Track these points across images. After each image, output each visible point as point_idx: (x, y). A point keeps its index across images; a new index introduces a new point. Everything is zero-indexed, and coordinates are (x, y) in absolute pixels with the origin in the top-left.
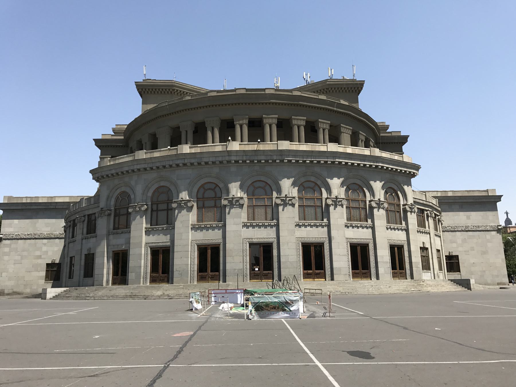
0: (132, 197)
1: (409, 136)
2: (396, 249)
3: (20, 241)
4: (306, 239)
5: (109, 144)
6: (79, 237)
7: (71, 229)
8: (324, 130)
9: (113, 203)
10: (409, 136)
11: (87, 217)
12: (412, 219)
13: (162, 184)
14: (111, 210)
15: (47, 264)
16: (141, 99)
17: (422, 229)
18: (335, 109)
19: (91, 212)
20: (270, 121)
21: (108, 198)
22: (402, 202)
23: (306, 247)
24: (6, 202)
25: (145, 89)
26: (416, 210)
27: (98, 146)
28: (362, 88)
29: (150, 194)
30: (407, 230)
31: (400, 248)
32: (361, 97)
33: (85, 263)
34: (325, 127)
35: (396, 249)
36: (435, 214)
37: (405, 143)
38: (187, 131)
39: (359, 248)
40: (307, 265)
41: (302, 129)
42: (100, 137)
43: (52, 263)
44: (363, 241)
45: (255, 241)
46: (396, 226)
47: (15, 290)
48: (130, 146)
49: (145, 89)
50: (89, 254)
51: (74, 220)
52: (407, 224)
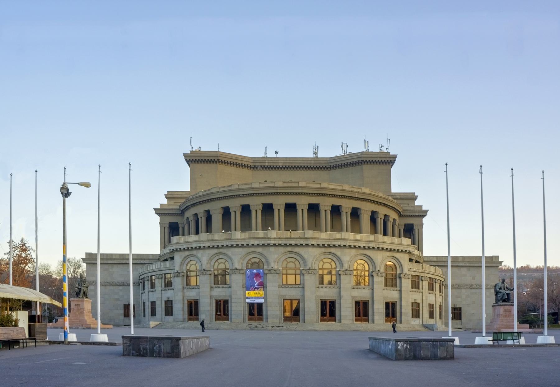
1: (428, 210)
5: (166, 212)
9: (184, 268)
10: (428, 210)
12: (406, 284)
16: (189, 168)
17: (414, 290)
21: (181, 264)
22: (398, 273)
23: (323, 303)
25: (195, 160)
26: (410, 277)
28: (395, 161)
29: (212, 264)
30: (400, 291)
31: (394, 304)
32: (395, 170)
37: (425, 216)
42: (158, 207)
44: (365, 299)
46: (392, 288)
49: (195, 160)
52: (401, 287)
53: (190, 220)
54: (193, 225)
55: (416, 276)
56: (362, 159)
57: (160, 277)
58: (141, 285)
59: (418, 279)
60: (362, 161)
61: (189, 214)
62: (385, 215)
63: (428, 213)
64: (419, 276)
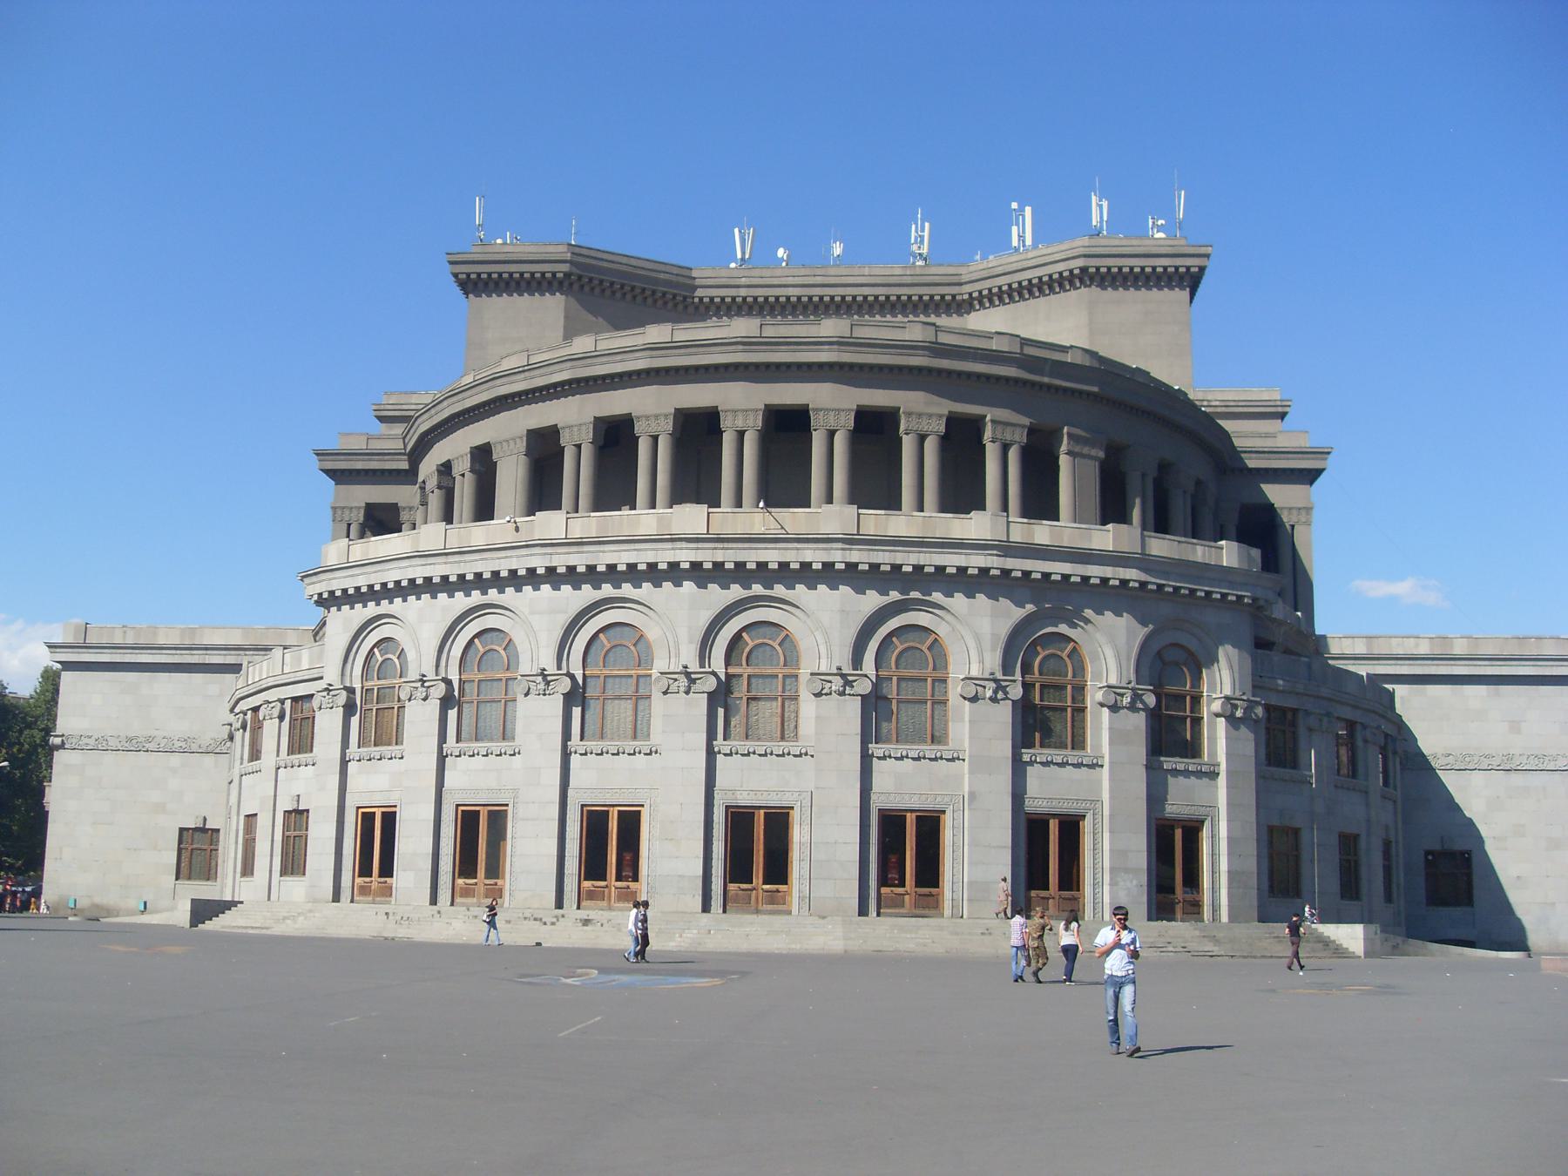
0: (411, 655)
2: (1178, 833)
3: (109, 757)
4: (892, 798)
5: (359, 465)
6: (268, 758)
7: (248, 734)
8: (1005, 448)
11: (288, 703)
13: (490, 621)
14: (351, 691)
15: (182, 830)
18: (1046, 380)
19: (300, 690)
20: (832, 422)
24: (70, 640)
27: (327, 472)
28: (1202, 269)
33: (286, 839)
34: (1008, 437)
35: (1178, 833)
36: (1351, 725)
37: (1319, 472)
38: (579, 447)
39: (1053, 825)
40: (890, 871)
41: (931, 446)
43: (196, 829)
45: (744, 799)
47: (97, 900)
48: (420, 479)
50: (298, 812)
51: (256, 710)
53: (428, 487)
54: (435, 500)
55: (1283, 710)
56: (1080, 263)
57: (276, 712)
58: (243, 740)
59: (1294, 724)
60: (1084, 270)
61: (428, 467)
62: (1164, 468)
63: (1330, 464)
64: (1295, 711)
